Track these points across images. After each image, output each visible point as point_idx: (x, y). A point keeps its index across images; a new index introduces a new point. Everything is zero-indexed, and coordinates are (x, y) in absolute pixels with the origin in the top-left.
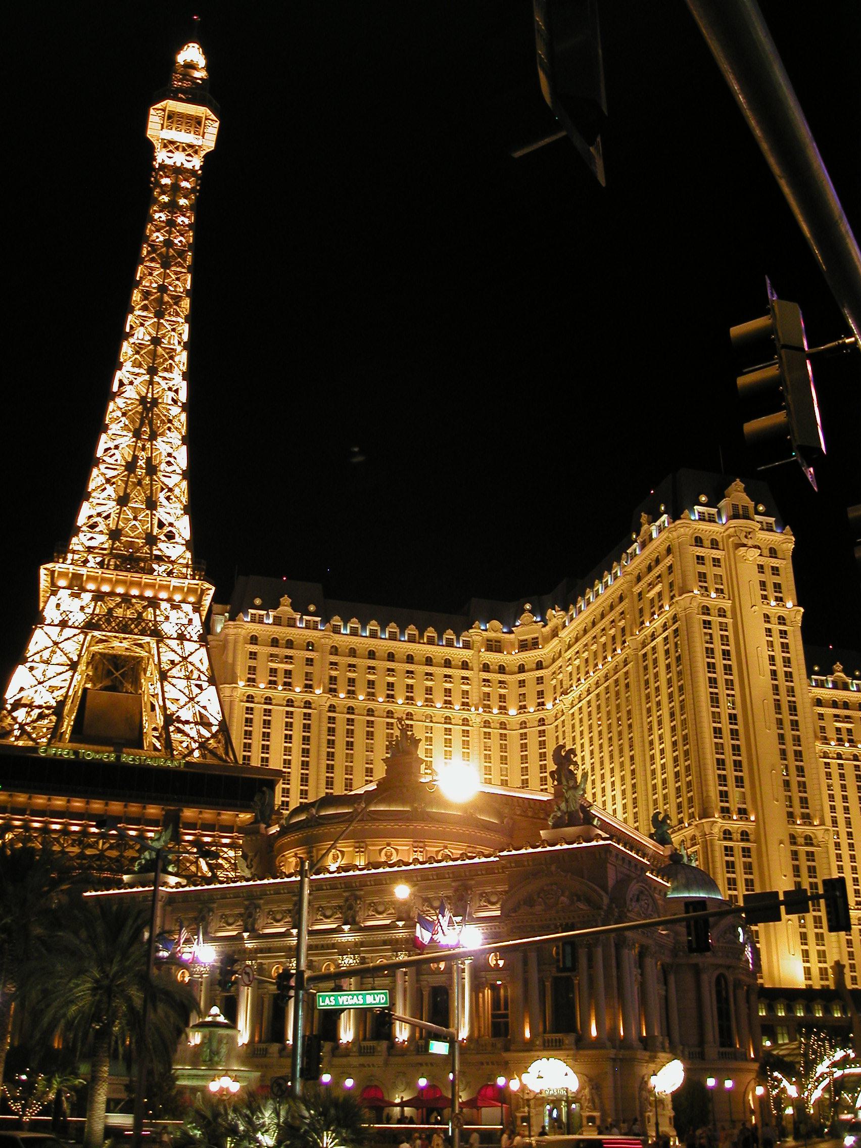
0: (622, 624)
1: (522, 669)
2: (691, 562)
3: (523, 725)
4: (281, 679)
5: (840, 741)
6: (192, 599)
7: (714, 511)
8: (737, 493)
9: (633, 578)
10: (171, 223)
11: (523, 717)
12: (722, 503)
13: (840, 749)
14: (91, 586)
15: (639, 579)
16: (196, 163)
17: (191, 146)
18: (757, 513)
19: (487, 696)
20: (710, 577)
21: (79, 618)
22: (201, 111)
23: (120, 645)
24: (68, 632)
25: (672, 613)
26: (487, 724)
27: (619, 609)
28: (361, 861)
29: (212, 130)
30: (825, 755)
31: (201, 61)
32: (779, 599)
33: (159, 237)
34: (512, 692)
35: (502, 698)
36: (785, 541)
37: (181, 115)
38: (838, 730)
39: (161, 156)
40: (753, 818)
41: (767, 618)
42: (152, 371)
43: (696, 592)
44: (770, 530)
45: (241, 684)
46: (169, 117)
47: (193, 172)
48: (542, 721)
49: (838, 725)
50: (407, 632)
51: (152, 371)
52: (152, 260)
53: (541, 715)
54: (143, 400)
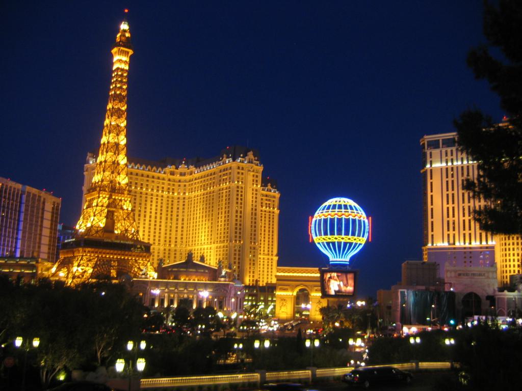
0: (214, 181)
1: (180, 181)
2: (236, 173)
3: (179, 198)
5: (266, 207)
7: (244, 159)
8: (251, 155)
9: (218, 170)
10: (121, 88)
11: (179, 196)
12: (246, 157)
13: (266, 209)
15: (221, 171)
16: (127, 68)
17: (126, 61)
18: (255, 160)
20: (240, 178)
21: (105, 205)
23: (112, 209)
24: (103, 208)
25: (229, 185)
26: (168, 197)
27: (213, 176)
28: (187, 279)
30: (262, 211)
32: (257, 185)
35: (173, 189)
36: (260, 168)
37: (123, 51)
38: (266, 204)
40: (242, 242)
41: (253, 190)
42: (118, 135)
43: (236, 182)
44: (257, 165)
47: (126, 70)
48: (184, 198)
49: (266, 202)
50: (148, 168)
53: (184, 196)
54: (115, 143)
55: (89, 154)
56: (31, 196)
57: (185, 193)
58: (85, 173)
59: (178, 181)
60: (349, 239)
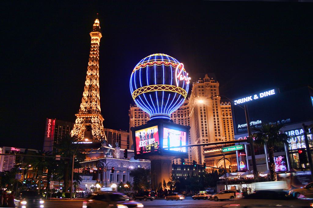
1: (185, 109)
4: (141, 116)
6: (97, 116)
8: (207, 77)
10: (94, 54)
11: (186, 118)
14: (82, 117)
17: (96, 39)
19: (179, 114)
22: (97, 32)
23: (88, 124)
24: (79, 124)
29: (100, 35)
31: (98, 22)
33: (92, 57)
34: (184, 113)
35: (182, 114)
37: (94, 34)
39: (92, 42)
45: (134, 118)
46: (93, 34)
48: (189, 118)
51: (91, 80)
52: (91, 61)
54: (90, 85)
55: (131, 104)
56: (108, 133)
57: (189, 115)
58: (129, 115)
59: (184, 109)
60: (149, 89)
